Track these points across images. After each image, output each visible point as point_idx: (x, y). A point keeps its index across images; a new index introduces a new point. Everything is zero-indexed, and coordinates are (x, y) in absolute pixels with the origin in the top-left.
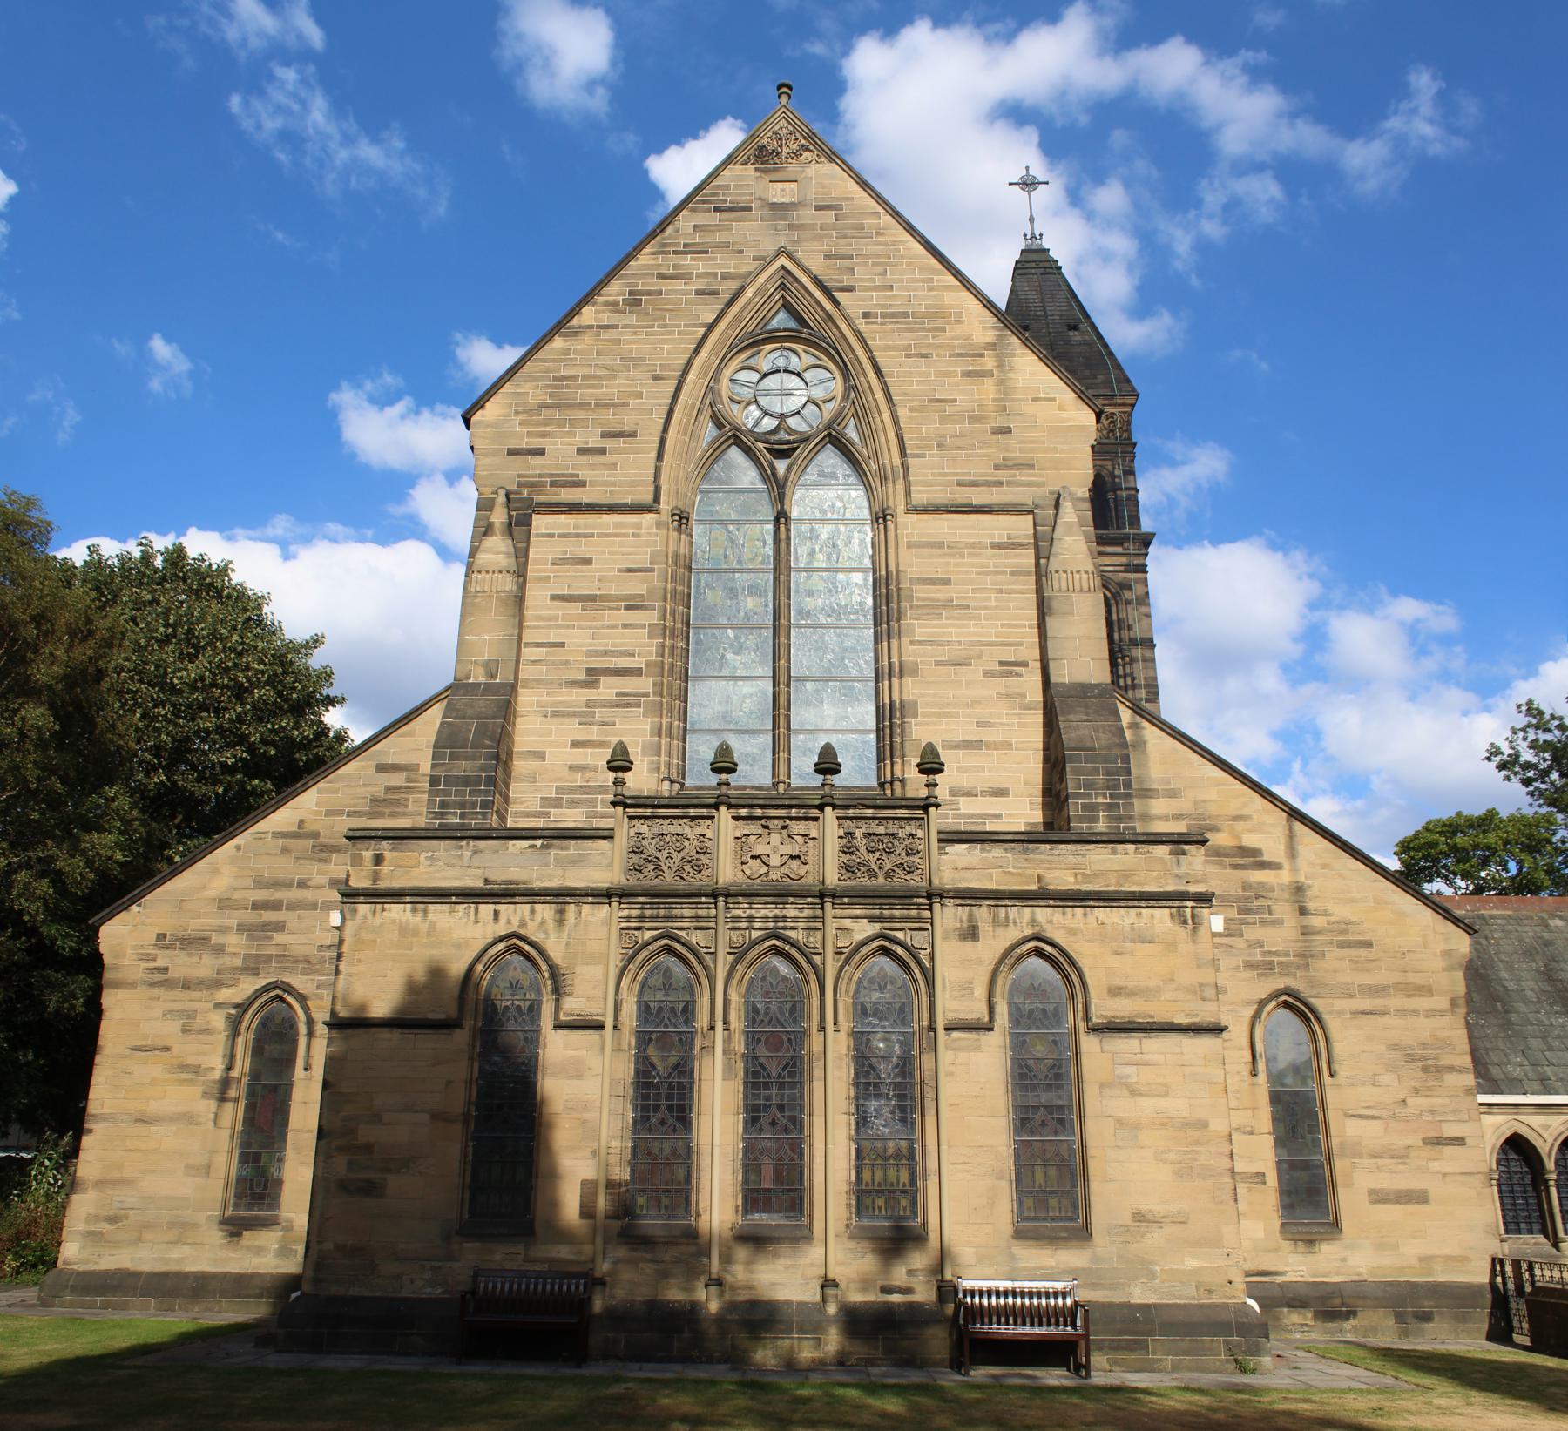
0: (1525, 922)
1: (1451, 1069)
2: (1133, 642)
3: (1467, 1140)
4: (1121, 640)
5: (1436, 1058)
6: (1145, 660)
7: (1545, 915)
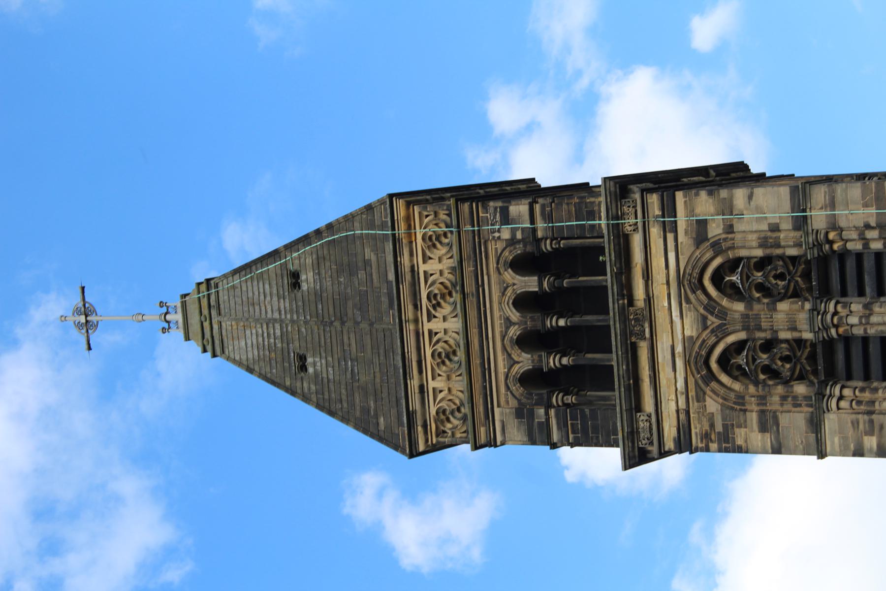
2: (801, 223)
4: (798, 245)
6: (832, 205)
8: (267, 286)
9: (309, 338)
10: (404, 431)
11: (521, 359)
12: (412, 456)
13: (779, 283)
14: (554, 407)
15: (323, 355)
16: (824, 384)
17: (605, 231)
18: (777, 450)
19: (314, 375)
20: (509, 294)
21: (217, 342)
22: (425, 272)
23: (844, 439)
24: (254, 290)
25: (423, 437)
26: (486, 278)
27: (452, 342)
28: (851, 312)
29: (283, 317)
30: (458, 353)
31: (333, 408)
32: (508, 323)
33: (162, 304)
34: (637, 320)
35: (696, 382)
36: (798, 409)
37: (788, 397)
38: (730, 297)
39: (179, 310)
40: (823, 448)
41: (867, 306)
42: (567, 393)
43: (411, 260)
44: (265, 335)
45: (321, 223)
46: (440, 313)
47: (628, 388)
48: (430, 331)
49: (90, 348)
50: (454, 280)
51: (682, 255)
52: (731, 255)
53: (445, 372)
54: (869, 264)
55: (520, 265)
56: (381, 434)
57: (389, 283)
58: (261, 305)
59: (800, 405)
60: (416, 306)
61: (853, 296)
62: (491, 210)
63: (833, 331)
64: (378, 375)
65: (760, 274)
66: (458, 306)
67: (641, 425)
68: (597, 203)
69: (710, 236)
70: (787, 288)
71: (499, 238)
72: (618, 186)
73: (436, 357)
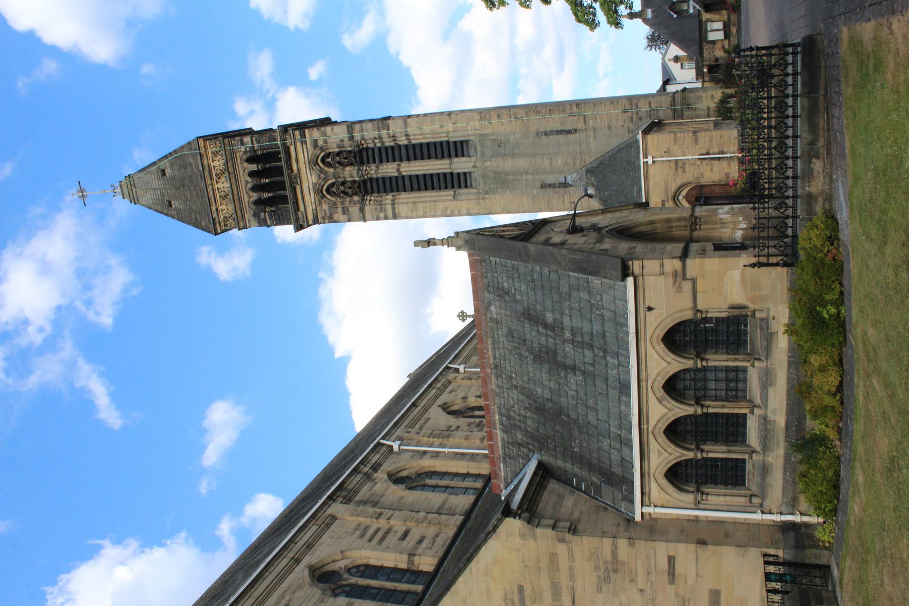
0: (496, 336)
1: (614, 553)
2: (351, 138)
3: (672, 554)
4: (351, 146)
5: (606, 562)
6: (362, 131)
16: (364, 196)
17: (280, 146)
18: (349, 220)
21: (136, 199)
23: (373, 215)
27: (226, 191)
31: (184, 219)
32: (247, 182)
33: (112, 186)
38: (328, 167)
39: (119, 187)
41: (377, 167)
42: (271, 207)
45: (171, 150)
46: (221, 181)
47: (294, 203)
49: (85, 205)
52: (327, 151)
54: (376, 152)
55: (250, 160)
57: (200, 171)
62: (236, 141)
63: (366, 177)
67: (300, 216)
69: (319, 145)
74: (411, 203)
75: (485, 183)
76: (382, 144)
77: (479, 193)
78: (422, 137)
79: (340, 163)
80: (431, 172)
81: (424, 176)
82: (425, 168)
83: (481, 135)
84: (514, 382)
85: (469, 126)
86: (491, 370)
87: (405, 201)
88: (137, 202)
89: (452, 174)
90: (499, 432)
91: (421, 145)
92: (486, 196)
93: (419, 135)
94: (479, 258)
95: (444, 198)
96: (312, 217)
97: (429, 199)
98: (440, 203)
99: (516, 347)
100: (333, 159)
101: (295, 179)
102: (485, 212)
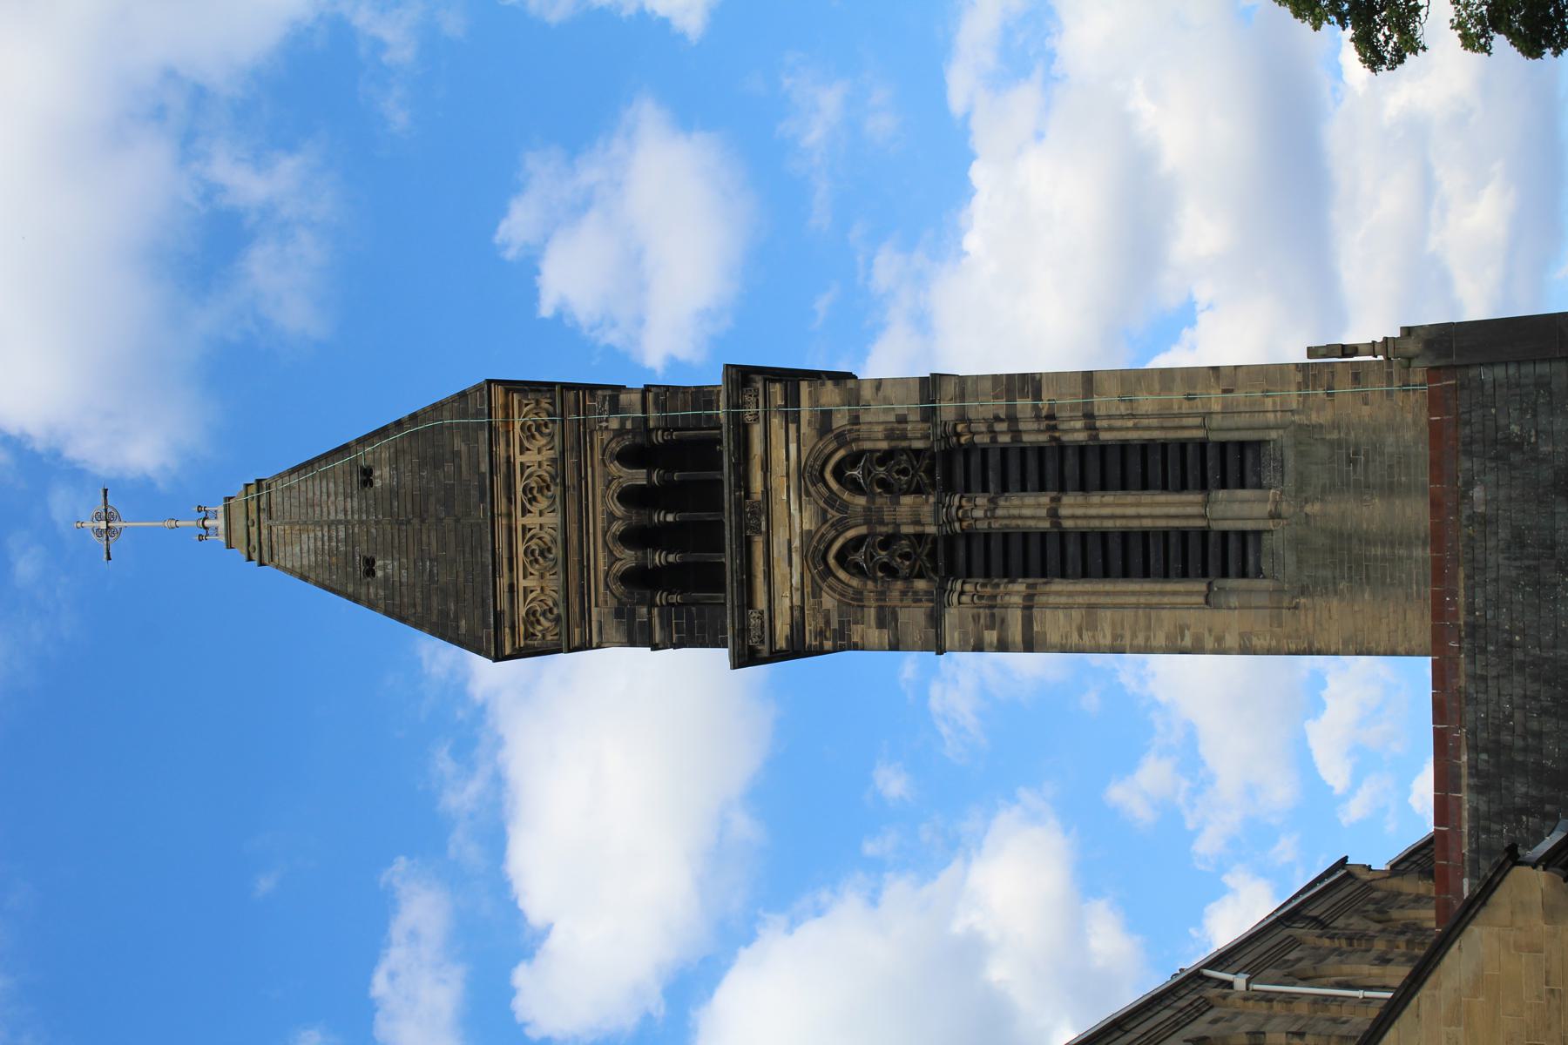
2: (929, 415)
4: (926, 437)
6: (962, 396)
7: (1466, 512)
8: (332, 485)
9: (380, 540)
10: (490, 634)
11: (623, 556)
12: (496, 659)
13: (902, 478)
14: (657, 606)
15: (396, 556)
16: (945, 579)
18: (895, 646)
19: (383, 579)
20: (614, 488)
21: (265, 549)
22: (522, 464)
23: (965, 634)
24: (315, 489)
25: (510, 640)
26: (589, 470)
27: (547, 538)
28: (976, 506)
29: (349, 517)
30: (554, 551)
32: (612, 517)
33: (199, 509)
34: (753, 513)
35: (813, 577)
36: (919, 604)
37: (908, 592)
38: (850, 490)
39: (221, 515)
40: (943, 643)
41: (991, 501)
43: (507, 451)
44: (326, 538)
45: (404, 413)
46: (535, 508)
47: (740, 583)
48: (524, 527)
50: (554, 473)
51: (804, 446)
53: (538, 570)
54: (994, 460)
55: (629, 457)
56: (462, 638)
58: (323, 505)
59: (921, 600)
60: (510, 500)
61: (977, 492)
62: (600, 399)
63: (957, 525)
64: (462, 574)
65: (882, 469)
66: (558, 500)
68: (716, 391)
70: (909, 483)
71: (606, 428)
72: (740, 374)
73: (529, 555)
74: (1080, 606)
75: (1300, 561)
76: (1014, 440)
77: (1281, 591)
78: (1130, 423)
79: (885, 485)
80: (1147, 523)
81: (1125, 535)
82: (1131, 511)
83: (1300, 427)
84: (1519, 655)
85: (1269, 403)
86: (1460, 640)
87: (1063, 600)
88: (266, 559)
89: (1204, 533)
90: (1464, 795)
91: (1124, 446)
92: (1303, 600)
93: (1122, 417)
94: (1454, 382)
95: (1179, 599)
96: (787, 630)
97: (1133, 600)
98: (1165, 613)
99: (1528, 567)
100: (868, 472)
101: (754, 518)
102: (1293, 647)
